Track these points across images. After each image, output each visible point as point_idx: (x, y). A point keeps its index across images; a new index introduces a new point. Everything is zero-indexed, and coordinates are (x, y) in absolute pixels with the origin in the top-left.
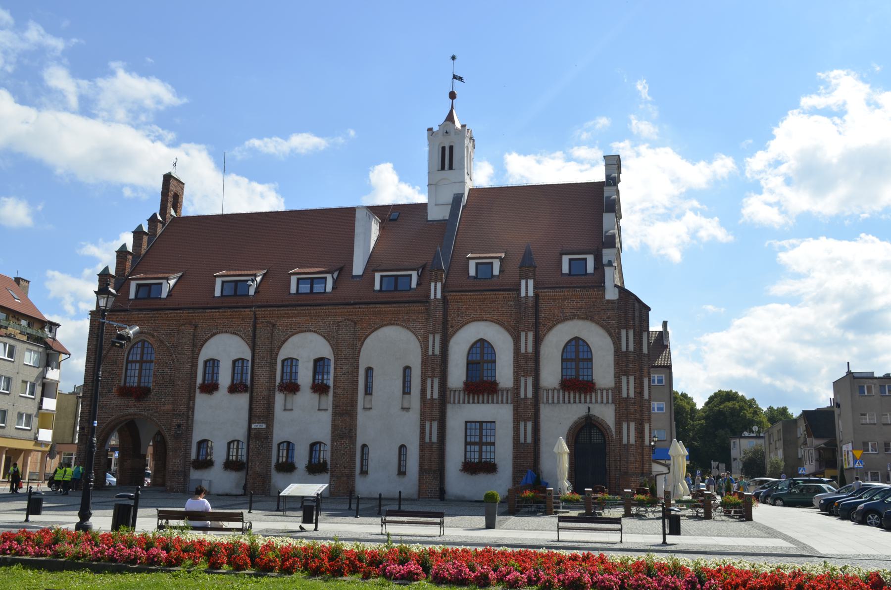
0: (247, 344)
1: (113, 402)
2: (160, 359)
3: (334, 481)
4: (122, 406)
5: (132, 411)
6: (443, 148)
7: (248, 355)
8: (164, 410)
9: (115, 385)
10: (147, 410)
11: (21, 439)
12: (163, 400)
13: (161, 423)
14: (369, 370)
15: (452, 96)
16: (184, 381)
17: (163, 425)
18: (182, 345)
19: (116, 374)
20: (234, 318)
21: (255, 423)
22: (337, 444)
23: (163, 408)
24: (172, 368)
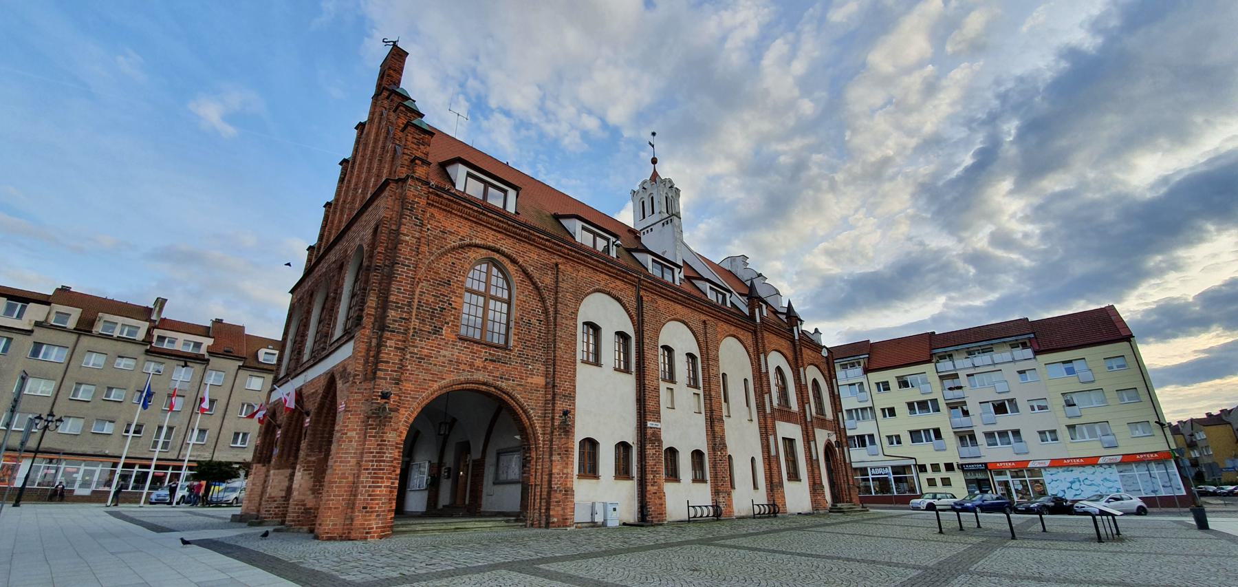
0: (631, 317)
1: (443, 352)
2: (524, 302)
3: (723, 497)
4: (460, 363)
5: (480, 376)
6: (666, 198)
7: (630, 330)
8: (532, 383)
9: (446, 323)
10: (505, 379)
11: (227, 408)
12: (530, 367)
13: (528, 405)
14: (724, 375)
15: (654, 161)
16: (568, 345)
17: (532, 409)
18: (562, 291)
19: (451, 304)
20: (617, 278)
21: (650, 421)
22: (721, 453)
23: (529, 380)
24: (541, 321)
